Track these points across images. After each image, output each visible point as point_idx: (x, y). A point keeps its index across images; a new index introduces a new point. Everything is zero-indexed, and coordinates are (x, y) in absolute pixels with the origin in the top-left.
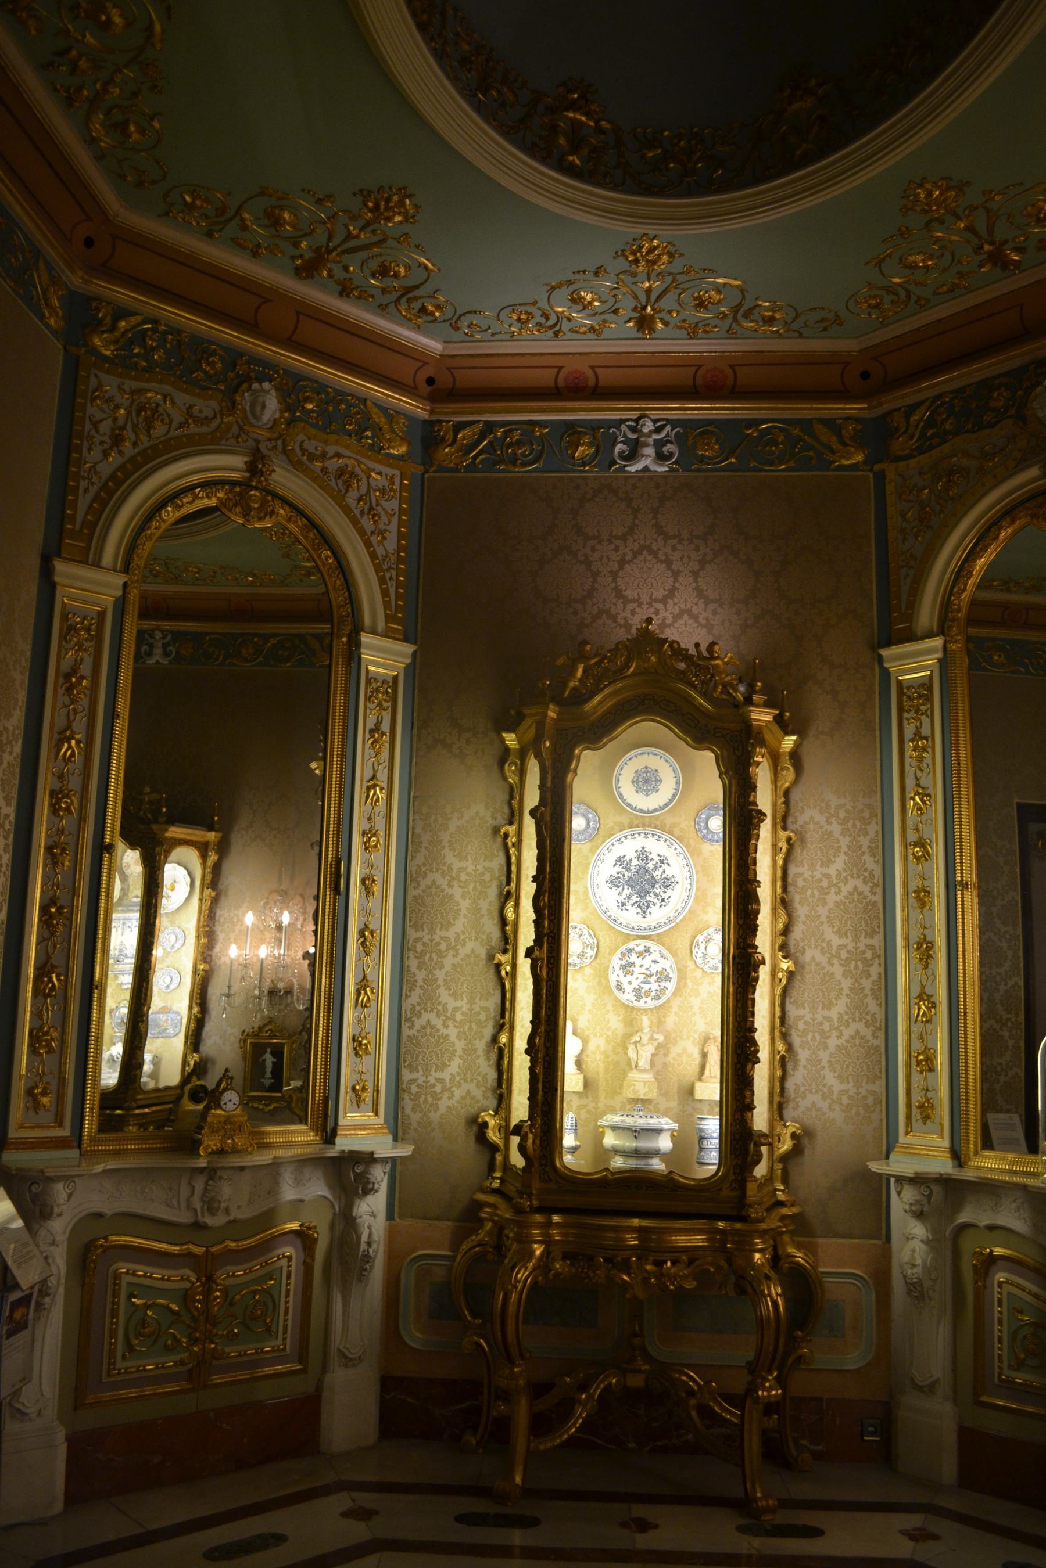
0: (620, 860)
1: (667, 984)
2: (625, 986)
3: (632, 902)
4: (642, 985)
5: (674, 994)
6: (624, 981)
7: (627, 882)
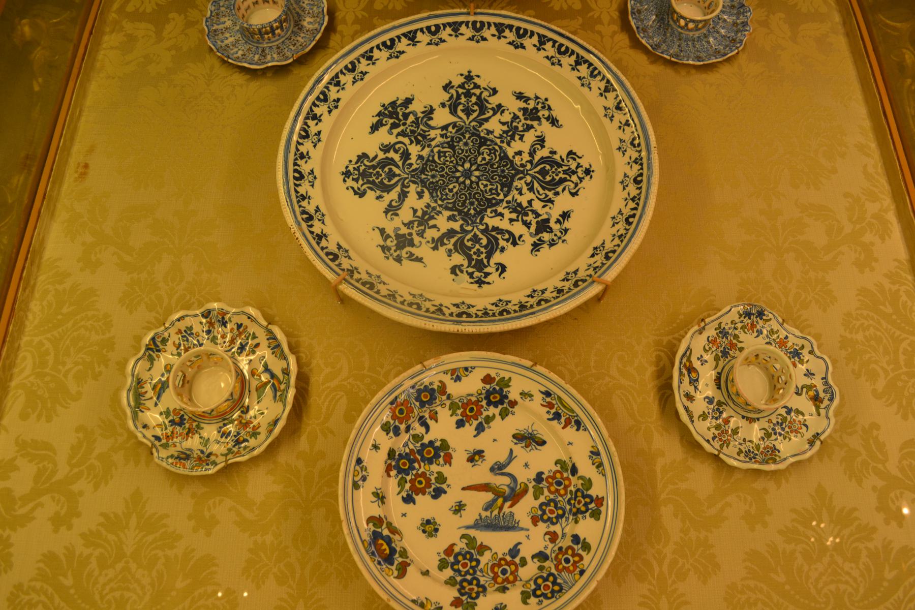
0: (392, 113)
1: (587, 528)
2: (412, 541)
3: (431, 234)
4: (483, 537)
5: (617, 573)
6: (406, 519)
7: (416, 176)
